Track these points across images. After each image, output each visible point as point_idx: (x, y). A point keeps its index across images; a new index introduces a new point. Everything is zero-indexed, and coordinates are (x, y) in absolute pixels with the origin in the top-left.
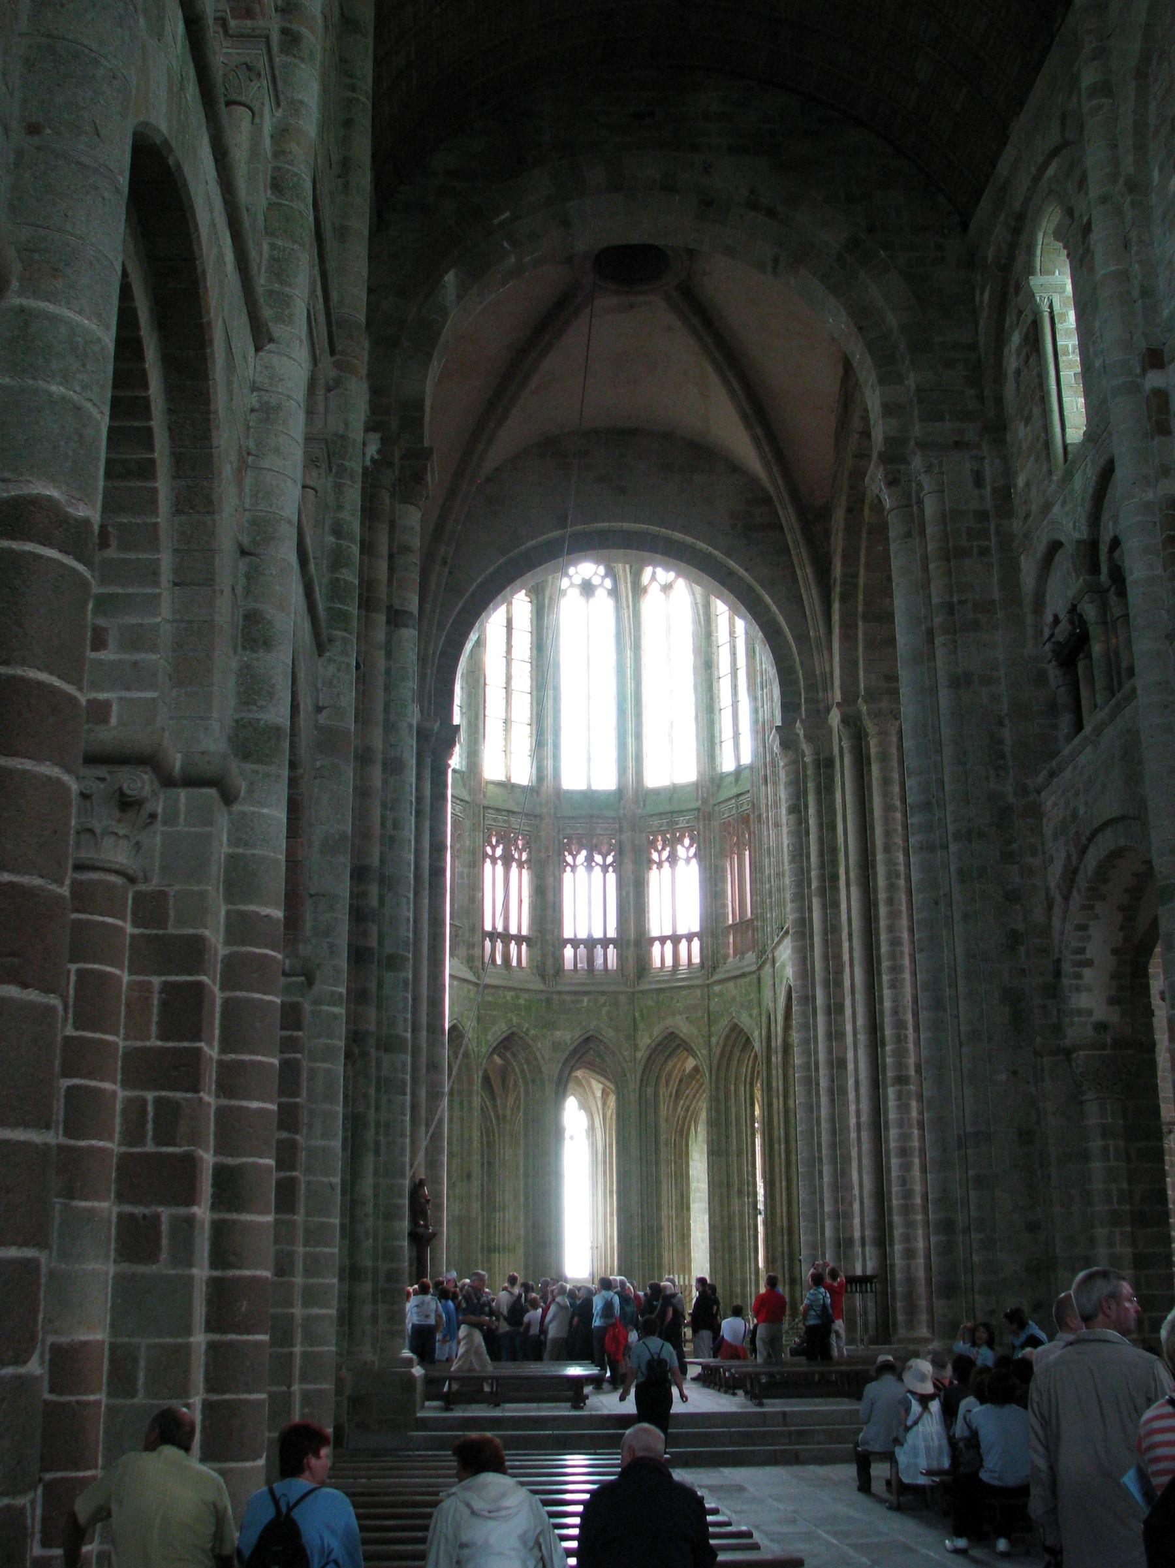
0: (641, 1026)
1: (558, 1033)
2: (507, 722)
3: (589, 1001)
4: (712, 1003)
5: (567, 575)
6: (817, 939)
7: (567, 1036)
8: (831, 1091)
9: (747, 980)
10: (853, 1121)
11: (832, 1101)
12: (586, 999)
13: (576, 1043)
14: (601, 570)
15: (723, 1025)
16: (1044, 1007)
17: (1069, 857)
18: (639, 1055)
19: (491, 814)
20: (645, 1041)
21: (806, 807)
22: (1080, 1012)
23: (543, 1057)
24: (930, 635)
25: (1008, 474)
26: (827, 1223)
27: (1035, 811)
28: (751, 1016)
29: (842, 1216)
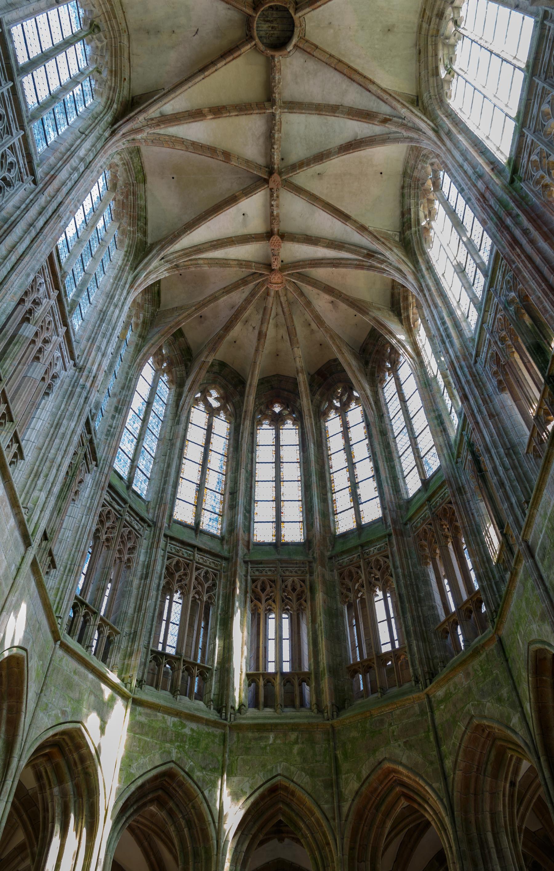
0: (345, 766)
2: (201, 488)
3: (275, 738)
4: (437, 714)
12: (272, 736)
19: (173, 547)
20: (351, 786)
28: (499, 700)
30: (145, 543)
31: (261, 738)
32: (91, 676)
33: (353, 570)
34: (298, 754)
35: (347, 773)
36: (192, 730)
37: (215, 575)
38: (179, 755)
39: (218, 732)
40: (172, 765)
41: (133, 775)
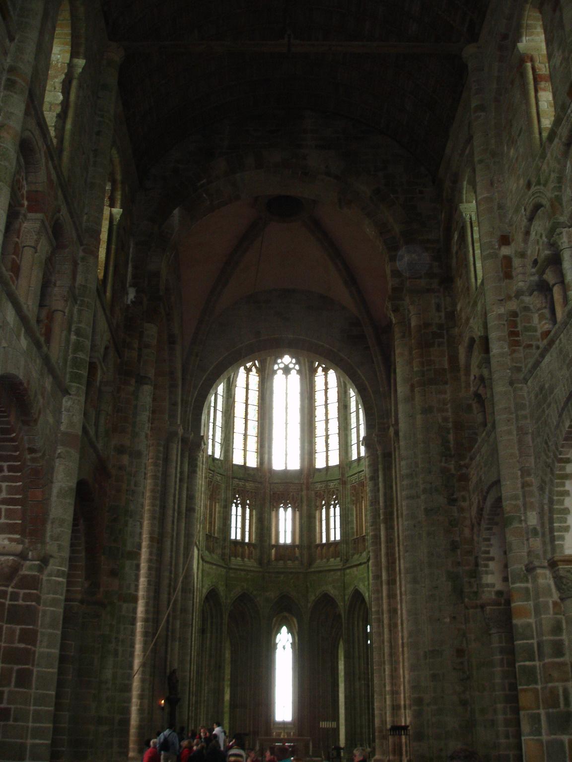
5: (276, 363)
6: (383, 546)
8: (390, 626)
9: (363, 566)
10: (400, 642)
11: (390, 631)
14: (294, 361)
15: (350, 591)
16: (470, 582)
17: (479, 502)
18: (309, 605)
19: (236, 481)
20: (312, 598)
21: (378, 477)
22: (488, 585)
24: (412, 387)
25: (454, 305)
26: (388, 697)
27: (464, 478)
28: (364, 585)
29: (395, 693)
30: (223, 486)
32: (214, 567)
33: (322, 493)
37: (256, 493)
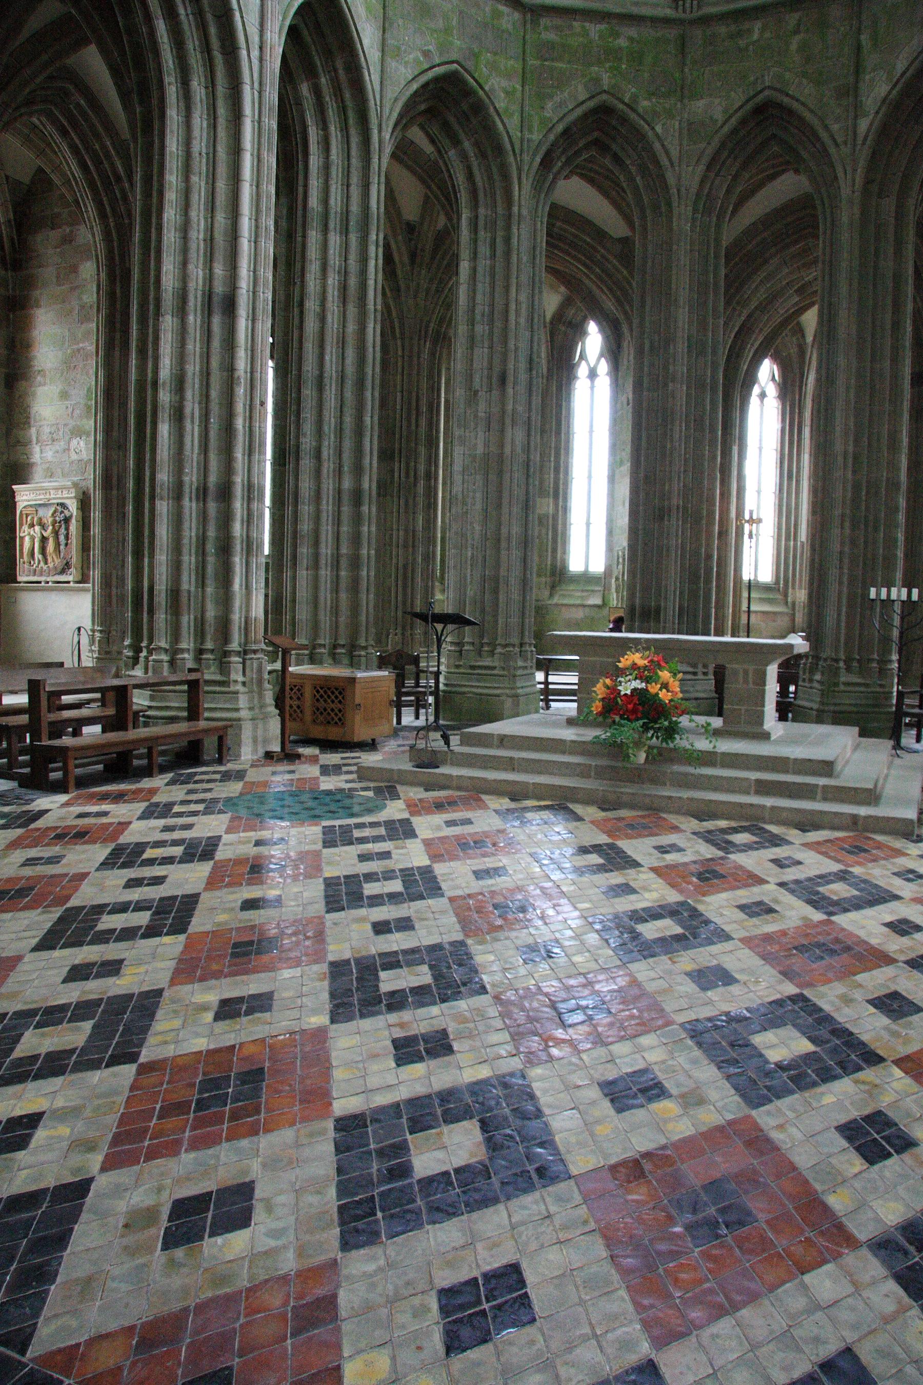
1: (699, 105)
3: (763, 30)
7: (717, 107)
13: (733, 121)
18: (863, 125)
23: (667, 153)
31: (739, 34)
34: (797, 51)
35: (874, 70)
36: (631, 39)
38: (613, 81)
39: (672, 33)
40: (604, 97)
41: (550, 119)
